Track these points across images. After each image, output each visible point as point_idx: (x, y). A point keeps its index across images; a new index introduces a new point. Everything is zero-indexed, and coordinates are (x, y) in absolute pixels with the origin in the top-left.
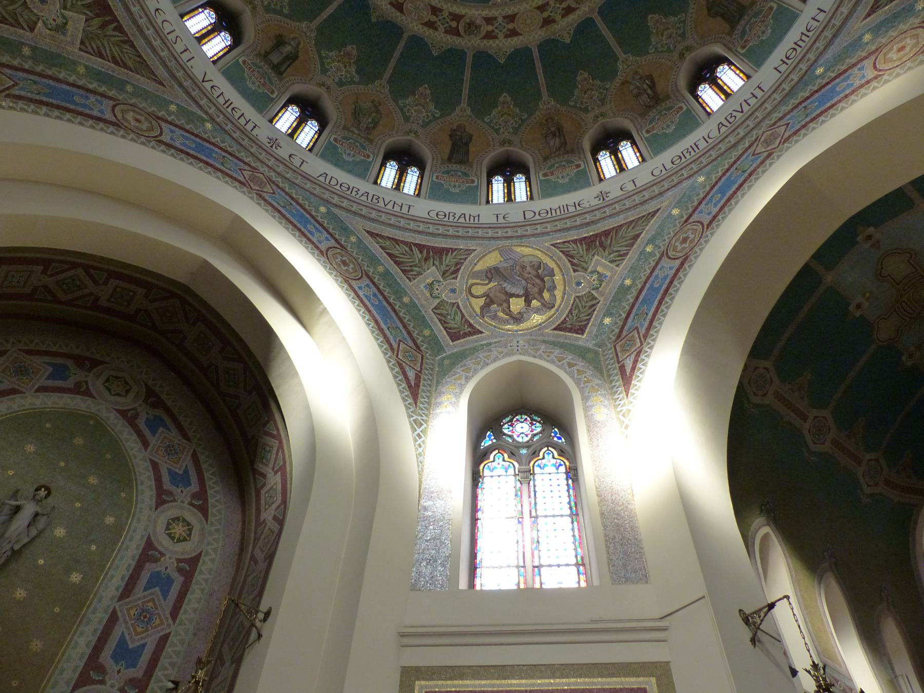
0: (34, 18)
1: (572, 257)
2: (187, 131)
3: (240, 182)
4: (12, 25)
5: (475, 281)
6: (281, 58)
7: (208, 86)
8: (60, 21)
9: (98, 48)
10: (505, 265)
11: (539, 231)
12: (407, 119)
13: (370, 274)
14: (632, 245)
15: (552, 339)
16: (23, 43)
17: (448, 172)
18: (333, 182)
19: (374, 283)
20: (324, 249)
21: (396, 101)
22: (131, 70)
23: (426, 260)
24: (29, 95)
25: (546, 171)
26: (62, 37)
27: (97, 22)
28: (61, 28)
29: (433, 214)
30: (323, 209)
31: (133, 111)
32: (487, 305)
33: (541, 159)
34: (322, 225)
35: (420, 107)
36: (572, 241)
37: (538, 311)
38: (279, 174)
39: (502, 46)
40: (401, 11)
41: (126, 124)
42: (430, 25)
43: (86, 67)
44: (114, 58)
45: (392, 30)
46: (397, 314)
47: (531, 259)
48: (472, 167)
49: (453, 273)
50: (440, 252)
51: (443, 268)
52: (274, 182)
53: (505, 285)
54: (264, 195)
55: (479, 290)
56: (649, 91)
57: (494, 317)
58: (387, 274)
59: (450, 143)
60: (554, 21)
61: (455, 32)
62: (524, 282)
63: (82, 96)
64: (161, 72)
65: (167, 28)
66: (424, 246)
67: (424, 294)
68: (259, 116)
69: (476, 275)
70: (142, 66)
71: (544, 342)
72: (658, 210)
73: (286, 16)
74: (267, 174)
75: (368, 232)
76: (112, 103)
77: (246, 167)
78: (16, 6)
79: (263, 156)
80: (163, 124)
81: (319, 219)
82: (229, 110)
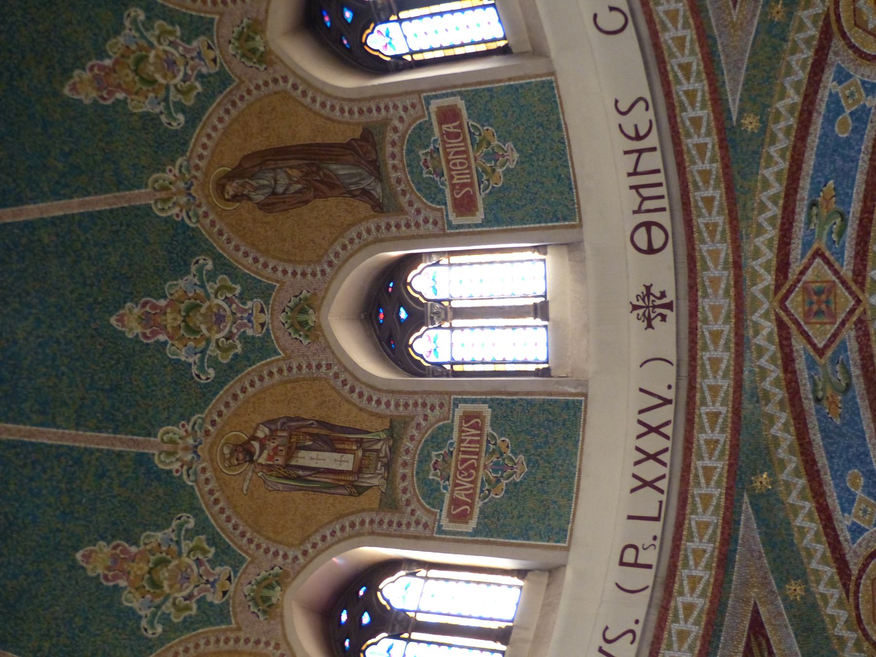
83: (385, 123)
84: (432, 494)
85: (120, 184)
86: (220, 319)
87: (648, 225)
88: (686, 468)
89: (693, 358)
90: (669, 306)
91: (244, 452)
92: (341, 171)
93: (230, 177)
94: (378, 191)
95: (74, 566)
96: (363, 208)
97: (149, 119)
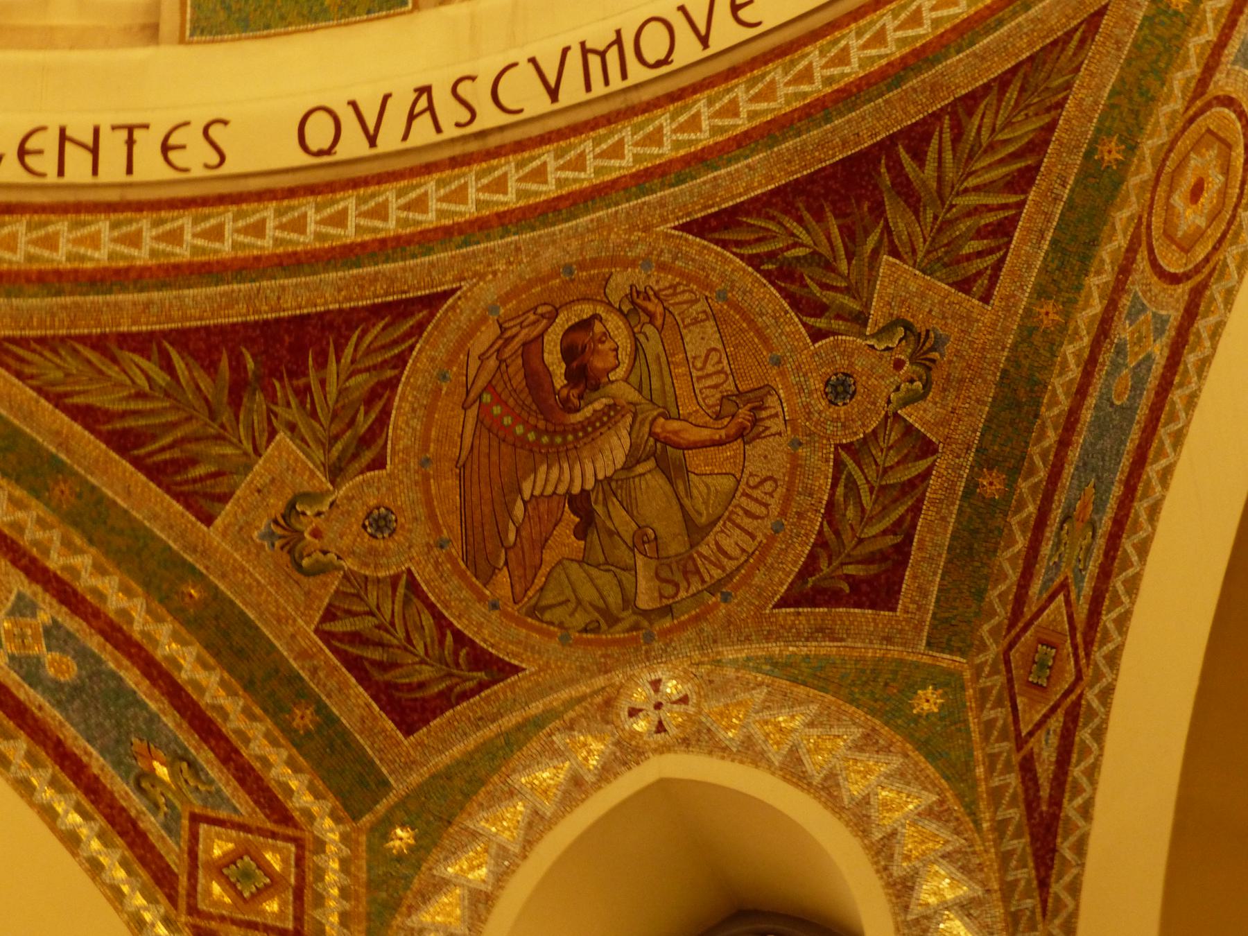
4: (916, 510)
9: (980, 234)
16: (969, 493)
22: (1051, 128)
24: (1093, 567)
26: (950, 348)
27: (899, 218)
28: (923, 347)
63: (1116, 366)
70: (1037, 77)
78: (861, 482)
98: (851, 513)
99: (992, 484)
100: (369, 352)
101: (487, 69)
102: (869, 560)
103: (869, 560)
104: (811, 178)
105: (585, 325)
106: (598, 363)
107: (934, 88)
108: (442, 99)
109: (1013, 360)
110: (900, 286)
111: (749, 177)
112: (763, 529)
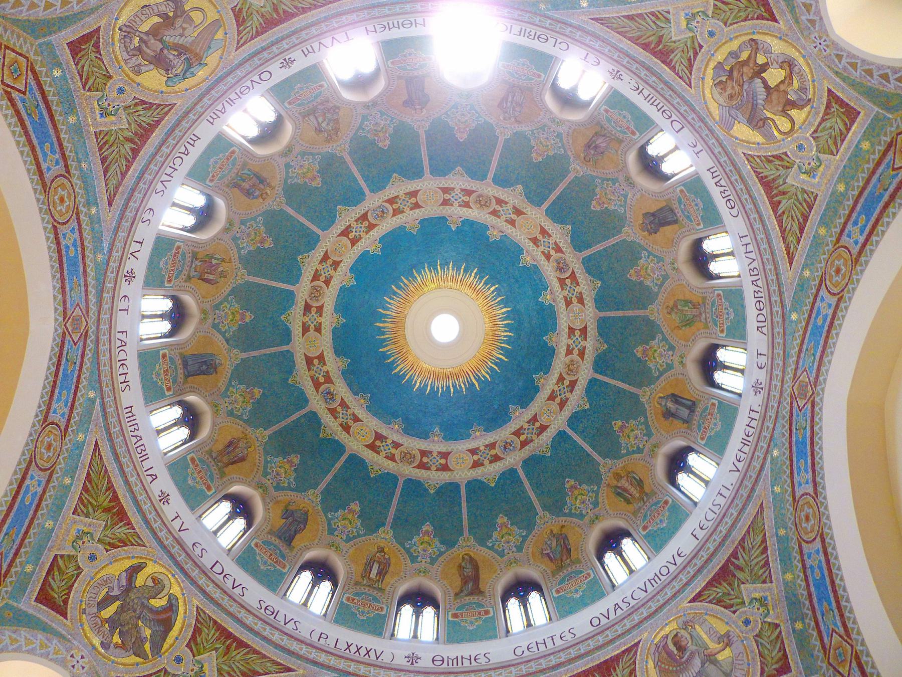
0: (767, 626)
1: (689, 60)
2: (792, 470)
3: (813, 406)
4: (783, 642)
5: (776, 133)
6: (684, 409)
7: (740, 466)
8: (757, 605)
10: (740, 115)
11: (686, 108)
12: (666, 277)
13: (834, 239)
14: (640, 16)
15: (789, 16)
17: (688, 217)
18: (761, 318)
19: (842, 231)
20: (835, 299)
21: (657, 294)
22: (765, 535)
23: (784, 193)
24: (838, 618)
25: (630, 135)
26: (769, 598)
27: (739, 574)
28: (763, 602)
29: (734, 212)
30: (794, 317)
31: (800, 524)
32: (793, 105)
33: (623, 145)
34: (811, 311)
35: (649, 271)
36: (674, 71)
37: (768, 52)
38: (784, 372)
39: (559, 234)
40: (585, 327)
41: (816, 528)
42: (581, 300)
43: (784, 573)
44: (763, 553)
45: (604, 326)
46: (864, 189)
47: (717, 96)
48: (670, 199)
49: (782, 160)
50: (767, 185)
51: (782, 171)
52: (795, 374)
53: (760, 102)
54: (812, 379)
55: (784, 124)
56: (510, 99)
57: (803, 89)
58: (824, 222)
59: (661, 229)
60: (514, 207)
61: (573, 276)
62: (745, 87)
63: (813, 572)
64: (752, 510)
65: (711, 516)
66: (771, 203)
67: (823, 174)
68: (740, 409)
69: (769, 137)
71: (797, 21)
72: (592, 19)
73: (646, 417)
74: (790, 384)
75: (791, 264)
76: (804, 545)
77: (795, 405)
79: (775, 393)
80: (798, 495)
81: (806, 316)
82: (750, 439)
83: (486, 597)
84: (357, 594)
85: (470, 529)
86: (425, 551)
87: (443, 661)
88: (352, 660)
89: (392, 669)
90: (412, 664)
91: (381, 550)
92: (470, 585)
93: (470, 557)
94: (462, 594)
95: (354, 500)
96: (457, 590)
97: (490, 537)
98: (766, 652)
99: (799, 626)
100: (626, 662)
101: (629, 594)
102: (776, 663)
103: (776, 663)
104: (714, 576)
105: (676, 635)
106: (683, 644)
107: (733, 542)
108: (621, 604)
109: (787, 593)
110: (750, 590)
111: (700, 583)
112: (745, 667)
